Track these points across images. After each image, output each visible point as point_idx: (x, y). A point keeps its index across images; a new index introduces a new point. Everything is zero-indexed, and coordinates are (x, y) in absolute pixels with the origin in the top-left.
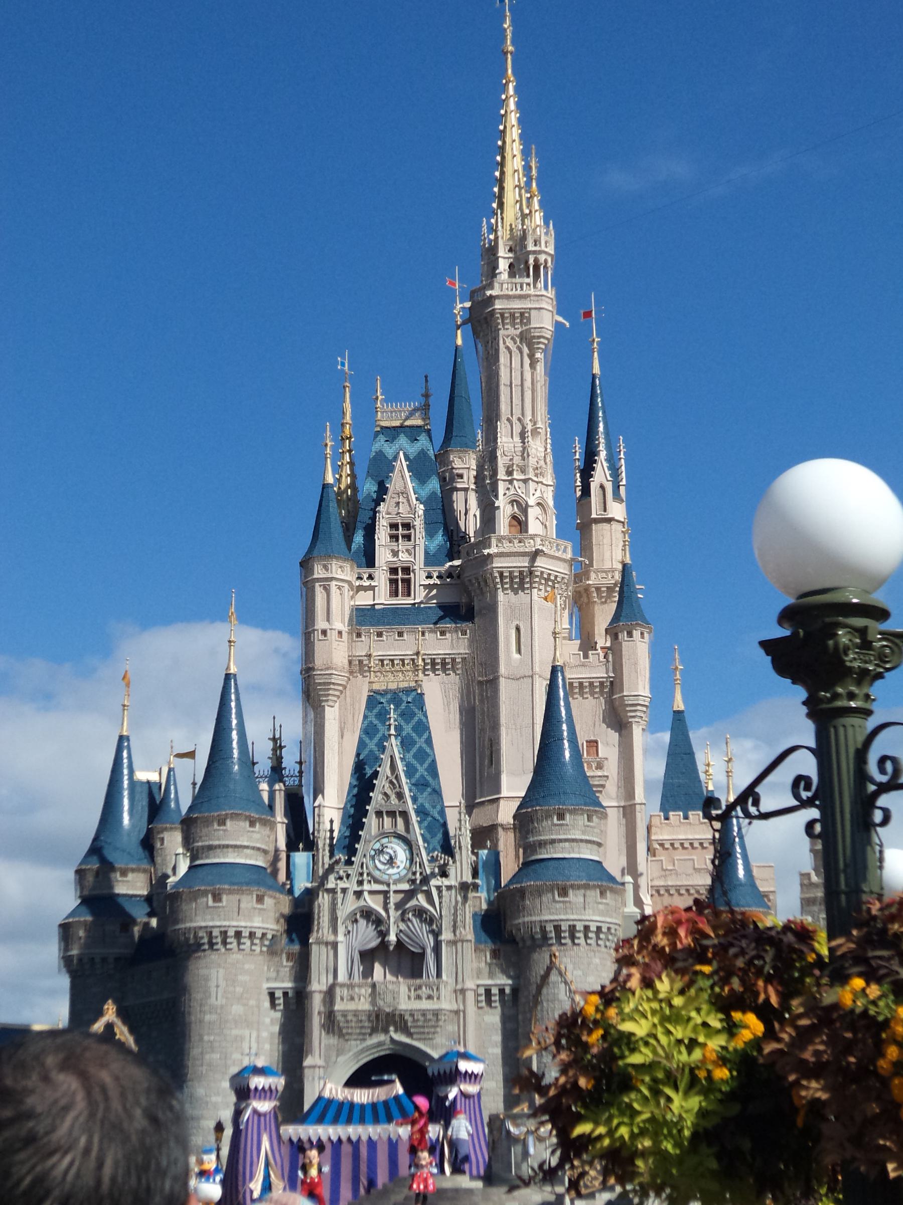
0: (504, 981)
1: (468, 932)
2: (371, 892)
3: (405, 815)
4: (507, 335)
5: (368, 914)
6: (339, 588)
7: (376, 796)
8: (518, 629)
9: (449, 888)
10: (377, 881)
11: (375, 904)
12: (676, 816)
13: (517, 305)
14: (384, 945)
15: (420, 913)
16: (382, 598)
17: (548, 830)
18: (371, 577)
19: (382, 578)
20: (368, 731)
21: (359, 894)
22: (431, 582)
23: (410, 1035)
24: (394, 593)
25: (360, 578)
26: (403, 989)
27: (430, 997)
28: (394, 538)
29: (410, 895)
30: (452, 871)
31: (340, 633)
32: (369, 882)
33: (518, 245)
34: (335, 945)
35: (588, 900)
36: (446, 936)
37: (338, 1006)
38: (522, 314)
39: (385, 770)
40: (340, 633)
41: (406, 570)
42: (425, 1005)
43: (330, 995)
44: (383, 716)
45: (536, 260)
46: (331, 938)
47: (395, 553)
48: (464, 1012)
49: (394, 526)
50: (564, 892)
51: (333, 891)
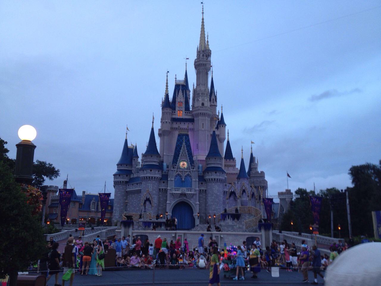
2: (179, 171)
6: (169, 114)
7: (181, 153)
8: (203, 124)
9: (194, 171)
10: (180, 169)
12: (228, 160)
18: (175, 112)
20: (178, 140)
22: (186, 114)
23: (187, 198)
25: (173, 112)
26: (186, 189)
27: (191, 191)
30: (195, 168)
31: (169, 122)
32: (179, 169)
35: (220, 175)
38: (205, 65)
40: (169, 122)
42: (189, 192)
44: (181, 138)
45: (208, 54)
46: (172, 179)
48: (197, 194)
51: (173, 170)
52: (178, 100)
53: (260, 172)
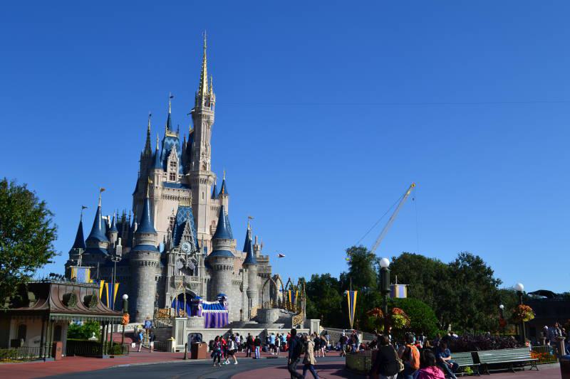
0: (209, 277)
1: (203, 263)
3: (191, 237)
4: (204, 120)
5: (181, 260)
7: (184, 233)
11: (183, 257)
13: (207, 114)
14: (184, 267)
15: (193, 261)
16: (168, 181)
17: (222, 243)
19: (168, 175)
21: (179, 255)
24: (171, 179)
28: (172, 165)
29: (191, 255)
33: (208, 98)
34: (174, 267)
36: (199, 266)
37: (176, 281)
39: (186, 226)
41: (174, 174)
43: (173, 278)
44: (182, 212)
47: (172, 169)
49: (172, 162)
50: (226, 258)
52: (170, 159)
53: (264, 257)
